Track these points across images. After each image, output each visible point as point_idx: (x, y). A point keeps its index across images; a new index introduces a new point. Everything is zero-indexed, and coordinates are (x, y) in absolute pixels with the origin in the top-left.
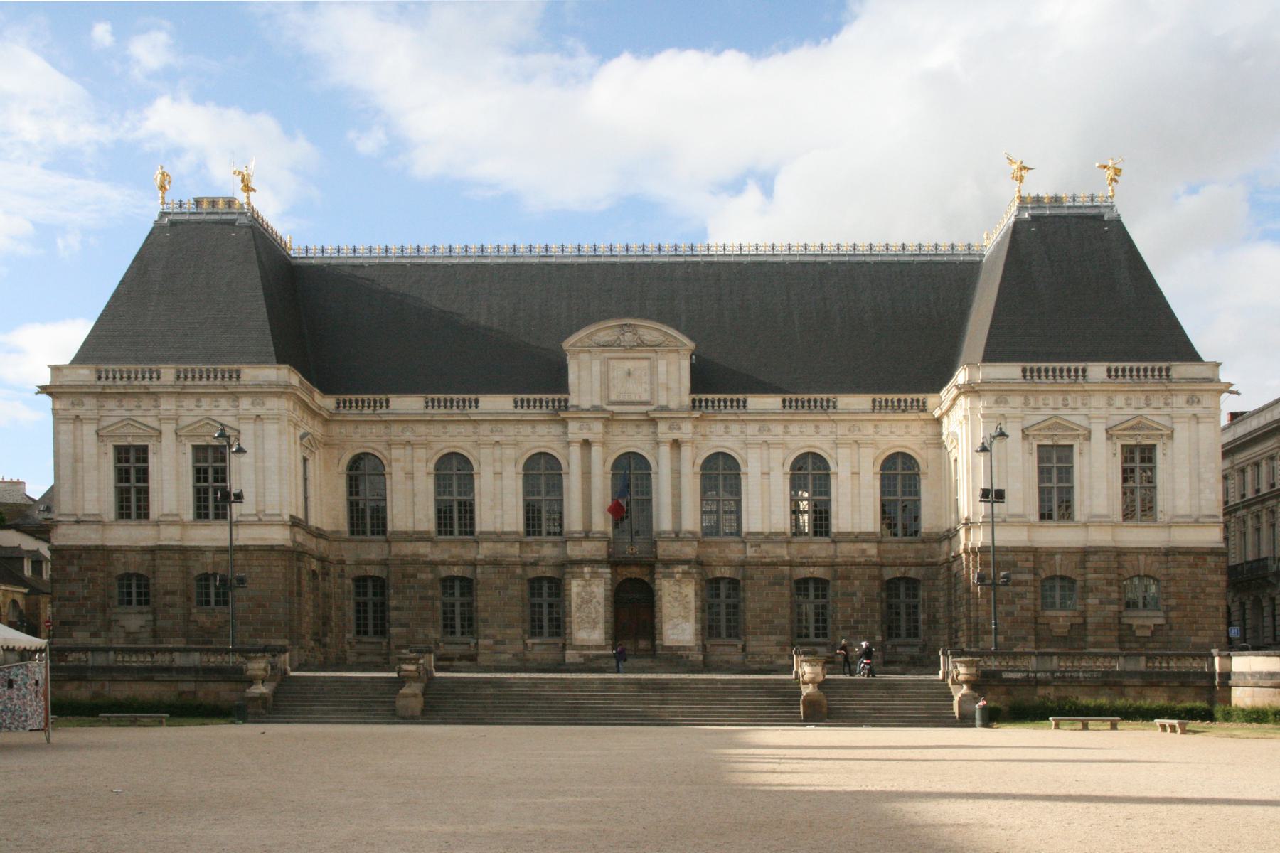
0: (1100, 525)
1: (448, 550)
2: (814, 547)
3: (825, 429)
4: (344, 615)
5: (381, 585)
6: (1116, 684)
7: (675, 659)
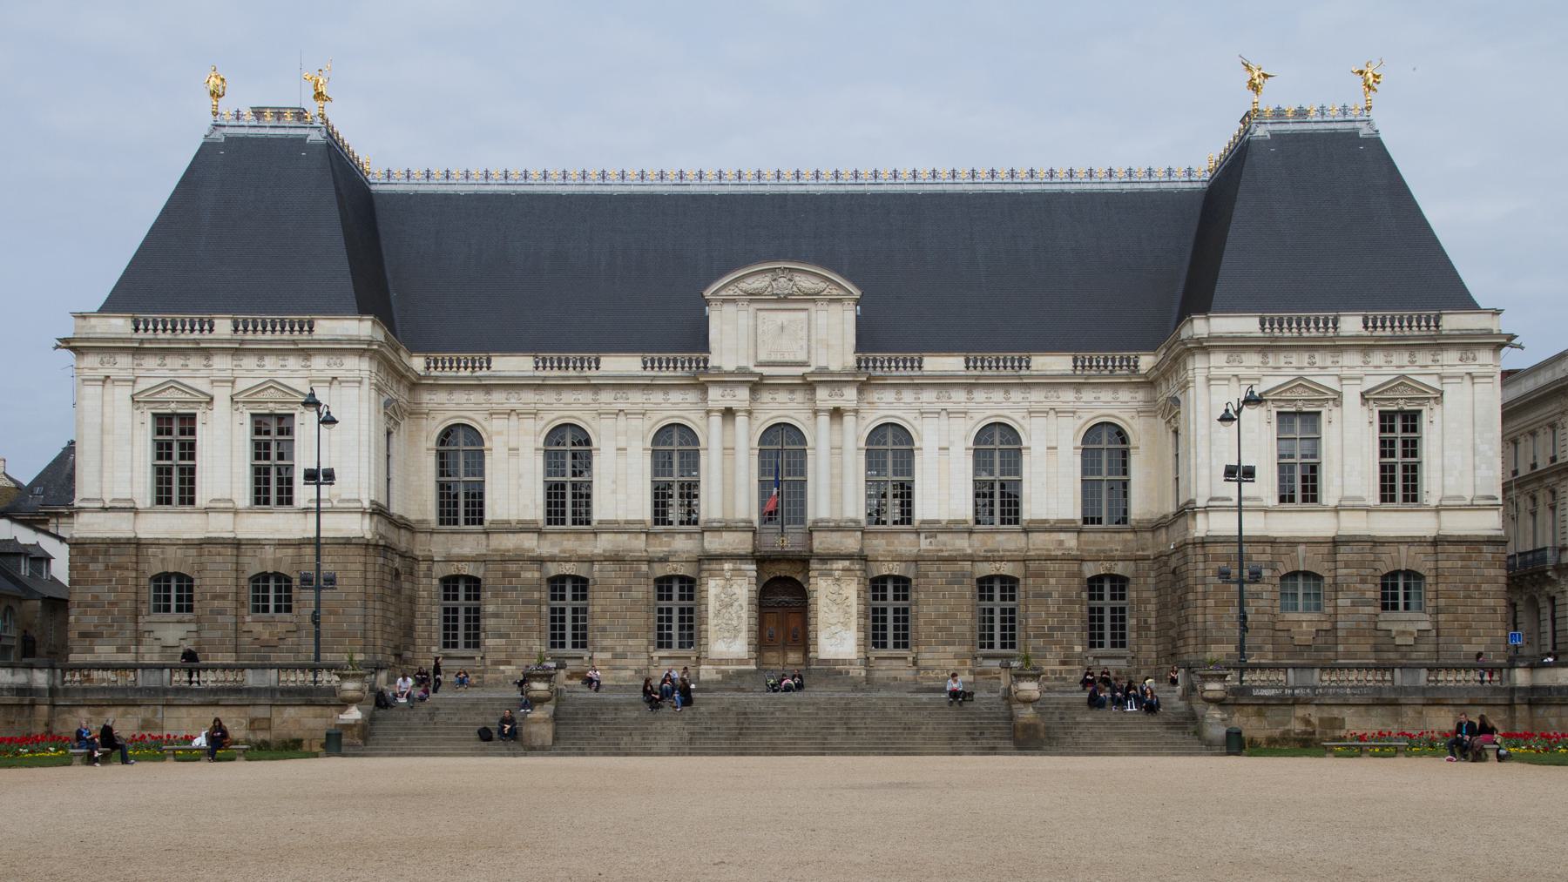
0: (1353, 509)
1: (561, 545)
2: (1000, 538)
3: (1016, 395)
4: (430, 624)
5: (474, 584)
6: (1394, 704)
7: (832, 671)
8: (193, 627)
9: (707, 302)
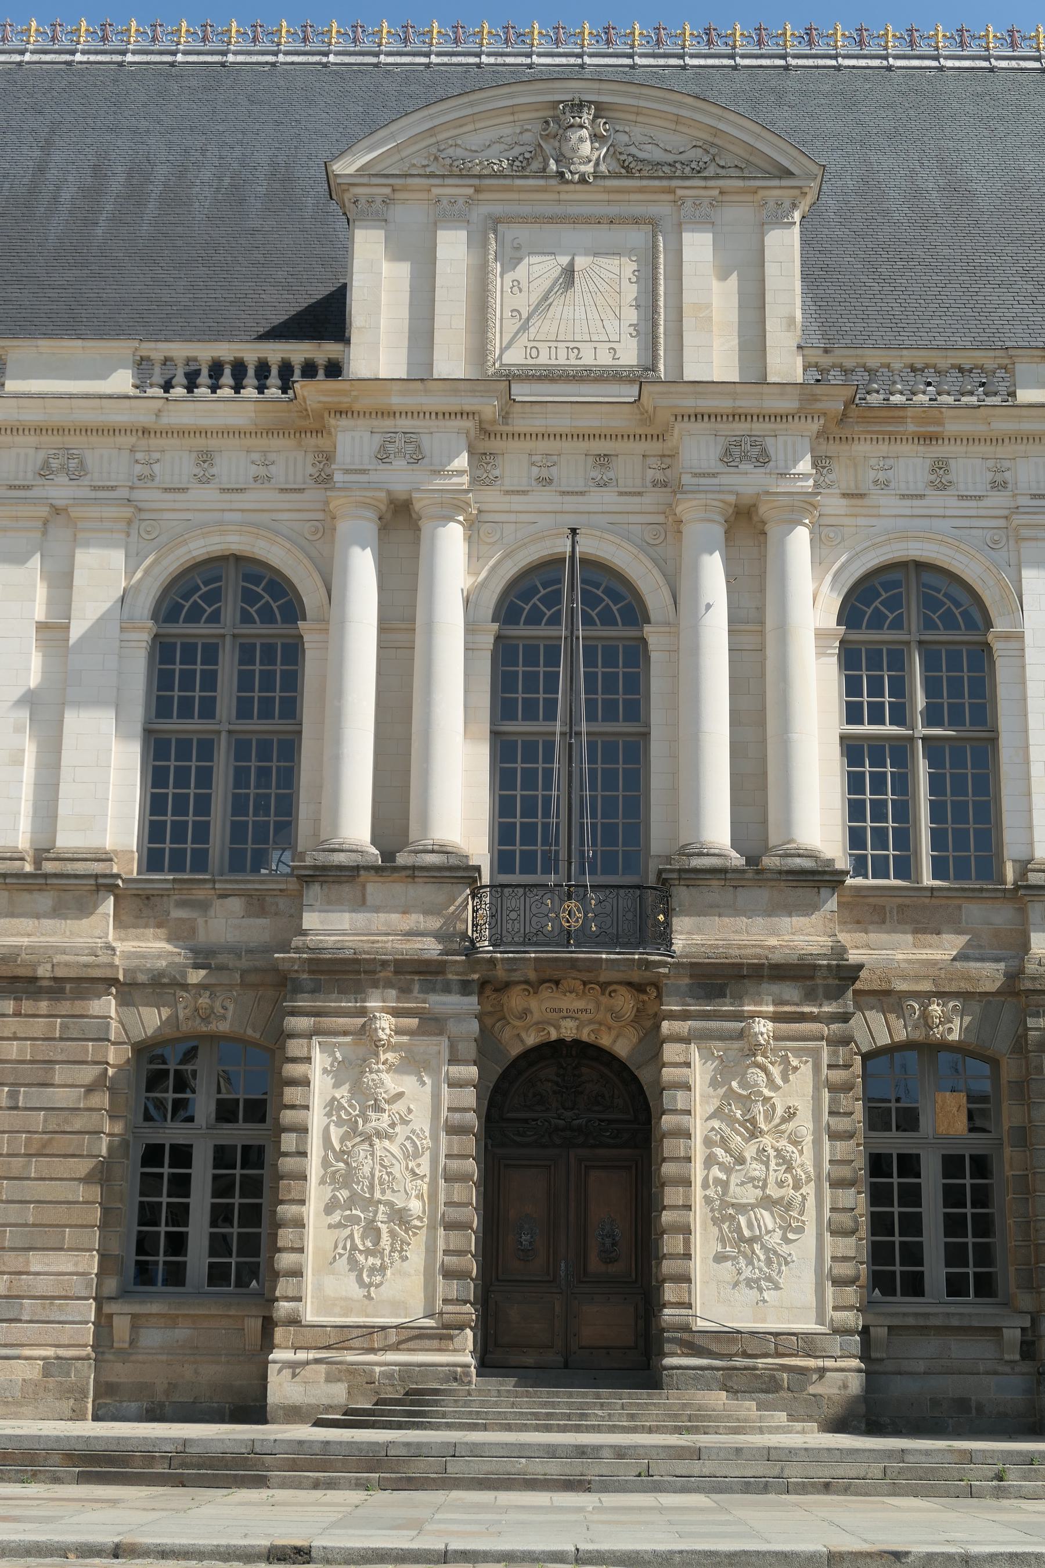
9: (341, 207)
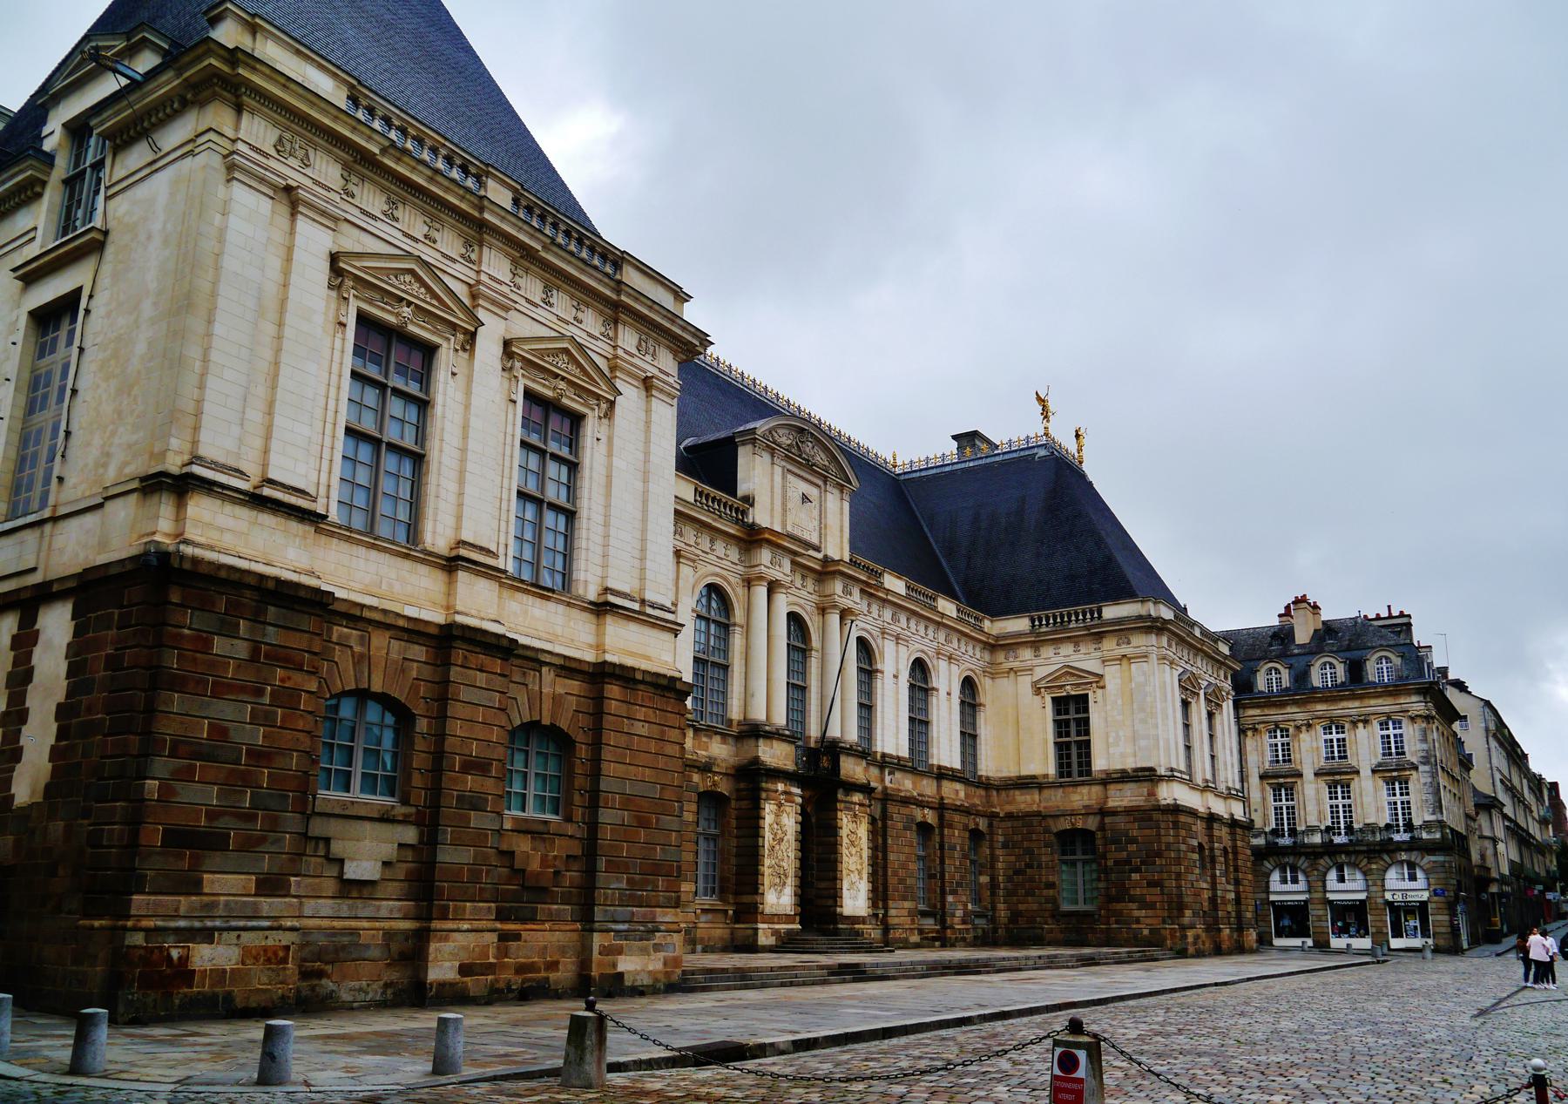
8: (410, 835)
